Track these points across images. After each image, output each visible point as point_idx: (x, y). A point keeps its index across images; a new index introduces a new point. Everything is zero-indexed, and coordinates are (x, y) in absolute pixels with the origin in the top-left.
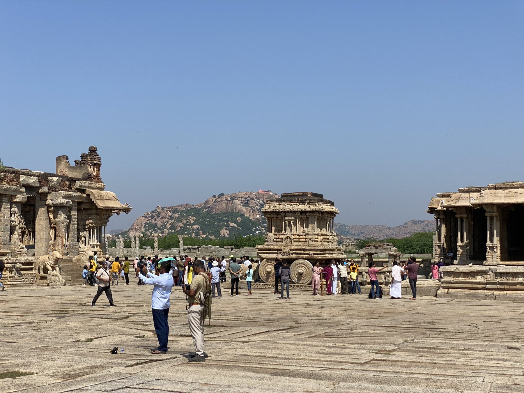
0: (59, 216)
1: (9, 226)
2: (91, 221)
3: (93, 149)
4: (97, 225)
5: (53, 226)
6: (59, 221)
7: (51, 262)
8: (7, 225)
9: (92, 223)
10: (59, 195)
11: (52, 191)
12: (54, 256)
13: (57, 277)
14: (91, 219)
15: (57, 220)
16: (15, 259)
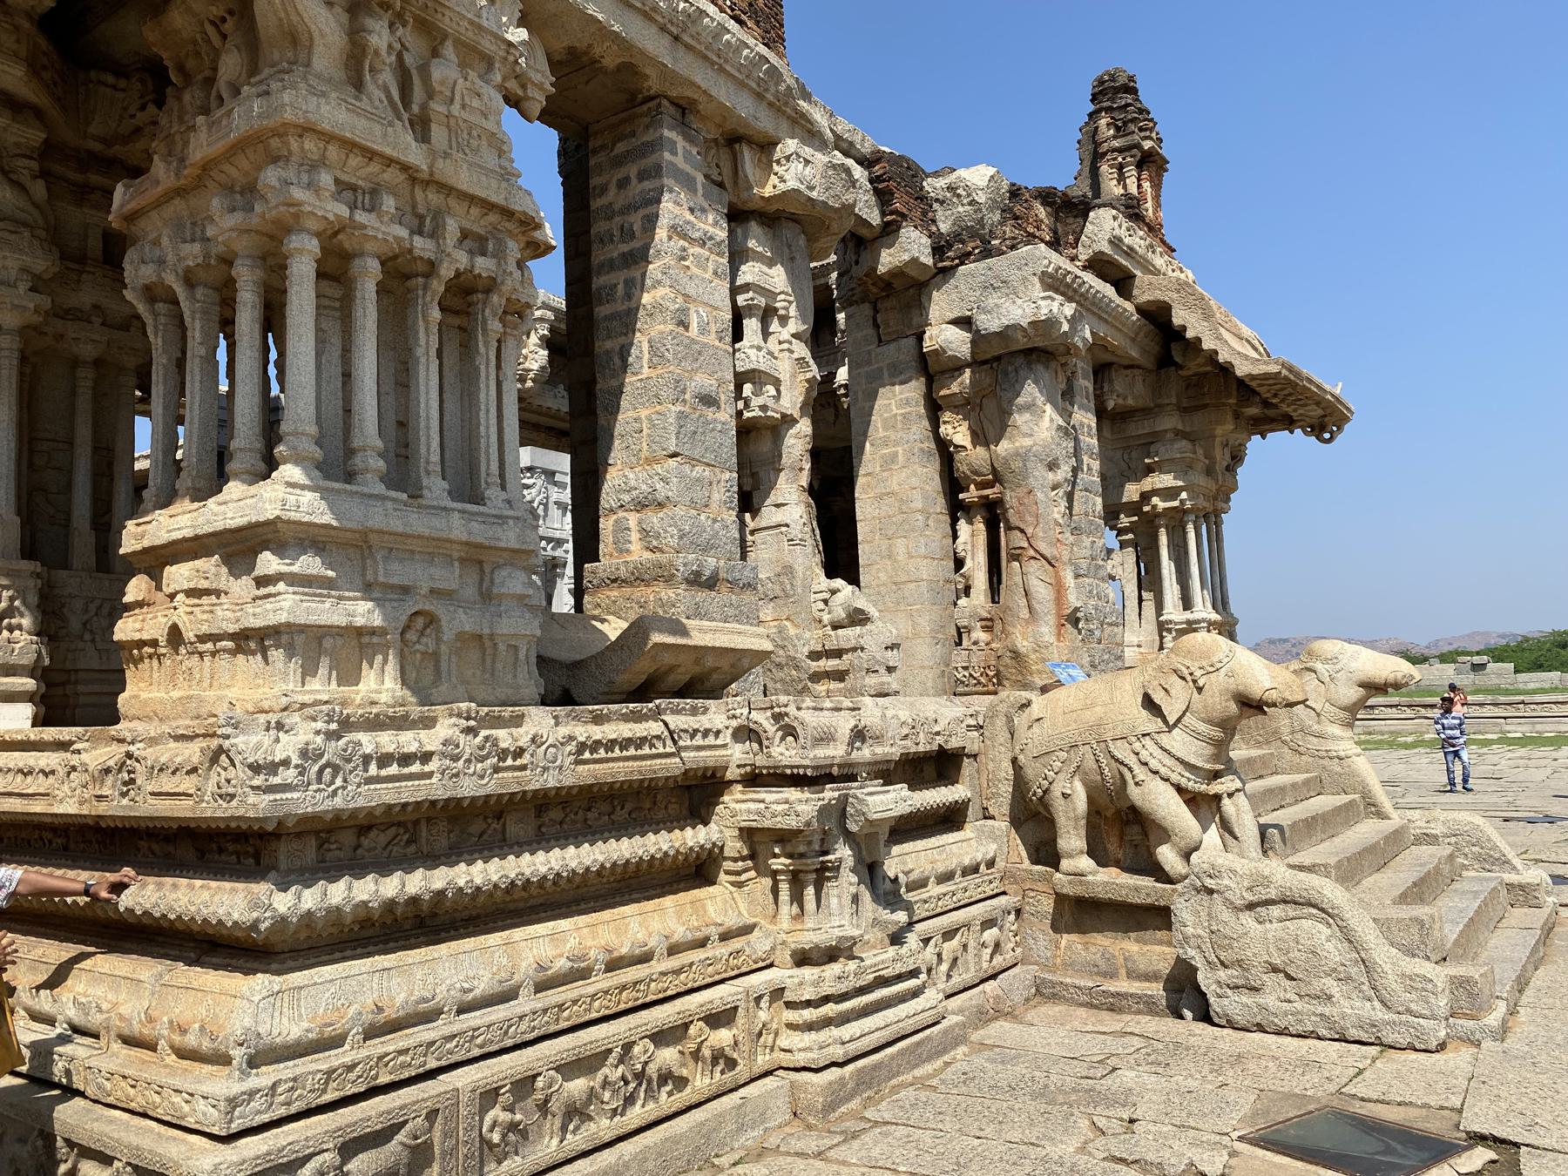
0: (1019, 419)
1: (725, 416)
2: (1166, 480)
3: (1122, 80)
4: (1202, 503)
5: (974, 499)
6: (1023, 455)
7: (1179, 742)
8: (708, 400)
9: (1170, 493)
10: (1014, 276)
11: (964, 258)
12: (1216, 684)
13: (1315, 931)
14: (1149, 470)
15: (1004, 448)
16: (844, 724)
